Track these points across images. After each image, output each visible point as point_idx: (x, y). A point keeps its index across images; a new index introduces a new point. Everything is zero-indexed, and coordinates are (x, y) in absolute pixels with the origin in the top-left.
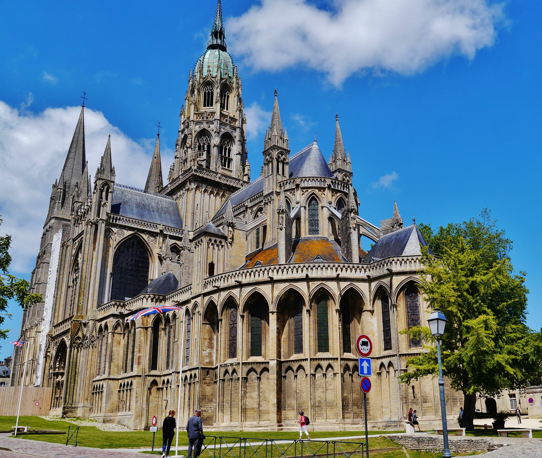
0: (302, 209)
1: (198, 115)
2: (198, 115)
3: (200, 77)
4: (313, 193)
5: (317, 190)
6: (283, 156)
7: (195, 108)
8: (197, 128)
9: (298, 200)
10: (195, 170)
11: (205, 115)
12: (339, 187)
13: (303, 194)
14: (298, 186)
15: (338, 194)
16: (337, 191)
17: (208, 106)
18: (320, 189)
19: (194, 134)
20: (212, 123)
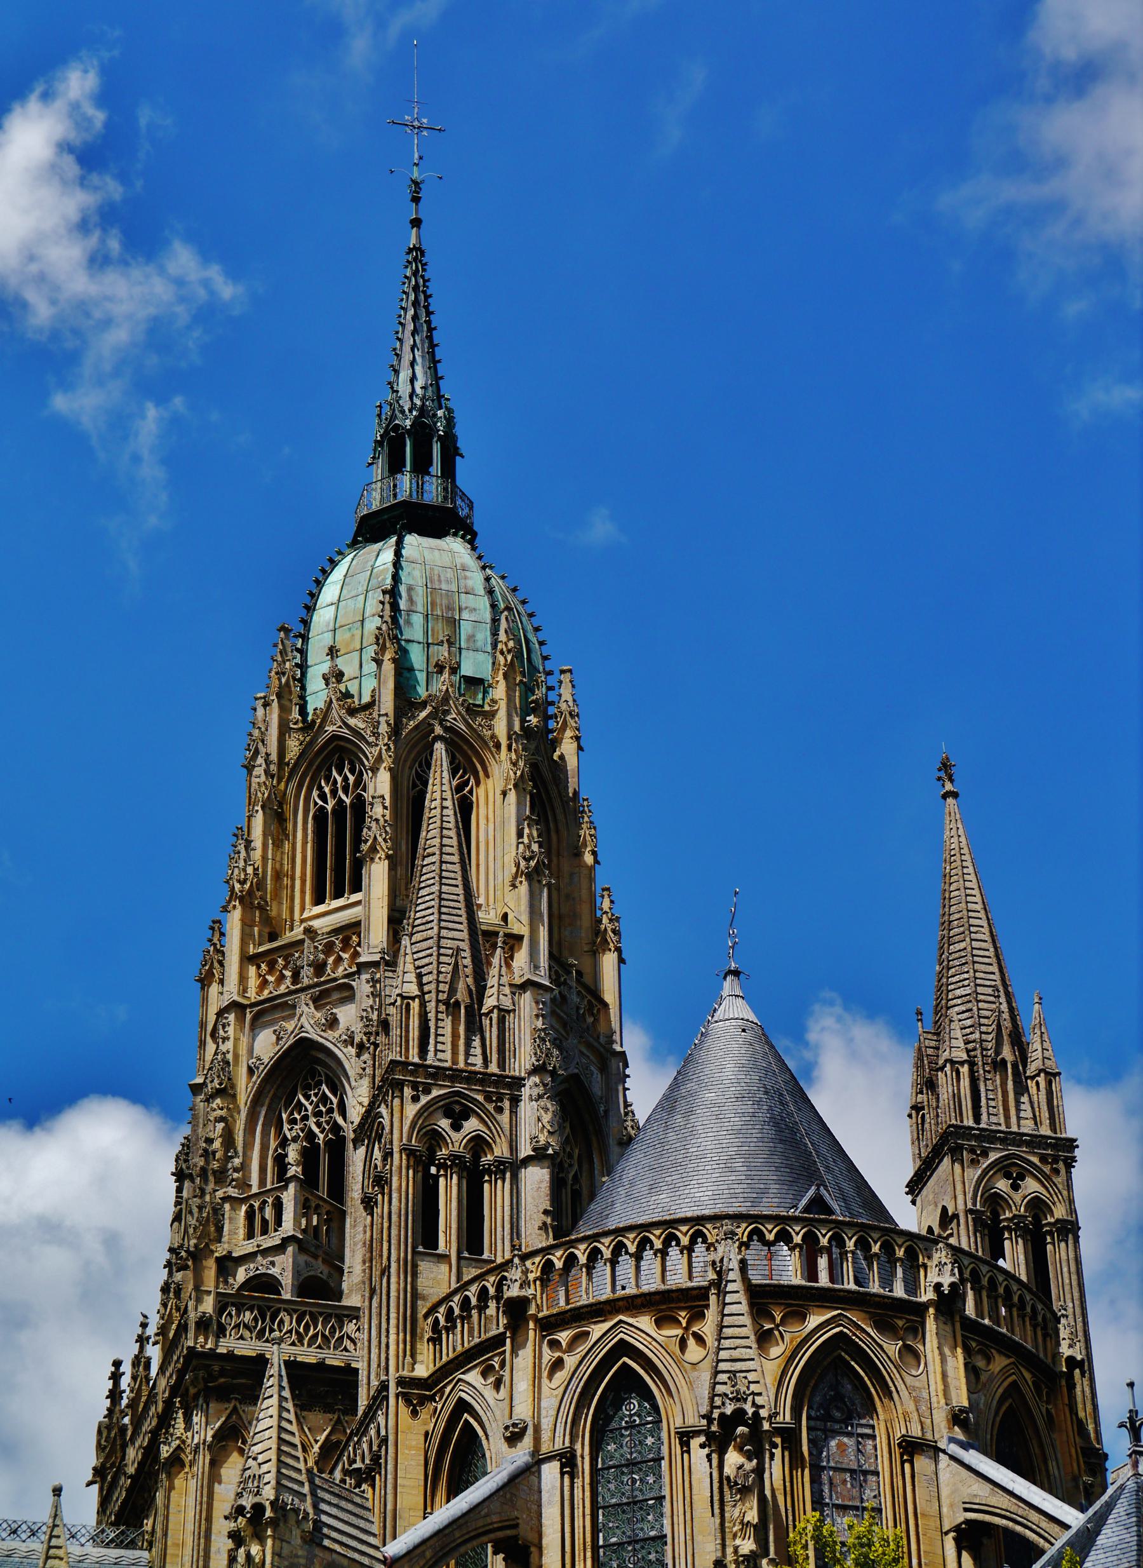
0: (550, 1472)
1: (272, 966)
2: (272, 966)
3: (284, 729)
4: (623, 1348)
5: (645, 1322)
6: (472, 1125)
7: (247, 925)
8: (267, 1045)
9: (523, 1411)
10: (203, 1325)
11: (308, 953)
12: (823, 1262)
13: (558, 1364)
14: (517, 1310)
15: (814, 1321)
16: (797, 1301)
17: (338, 894)
18: (665, 1305)
19: (244, 1088)
20: (347, 993)
